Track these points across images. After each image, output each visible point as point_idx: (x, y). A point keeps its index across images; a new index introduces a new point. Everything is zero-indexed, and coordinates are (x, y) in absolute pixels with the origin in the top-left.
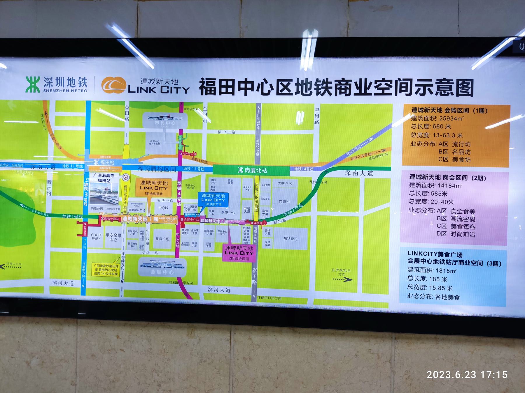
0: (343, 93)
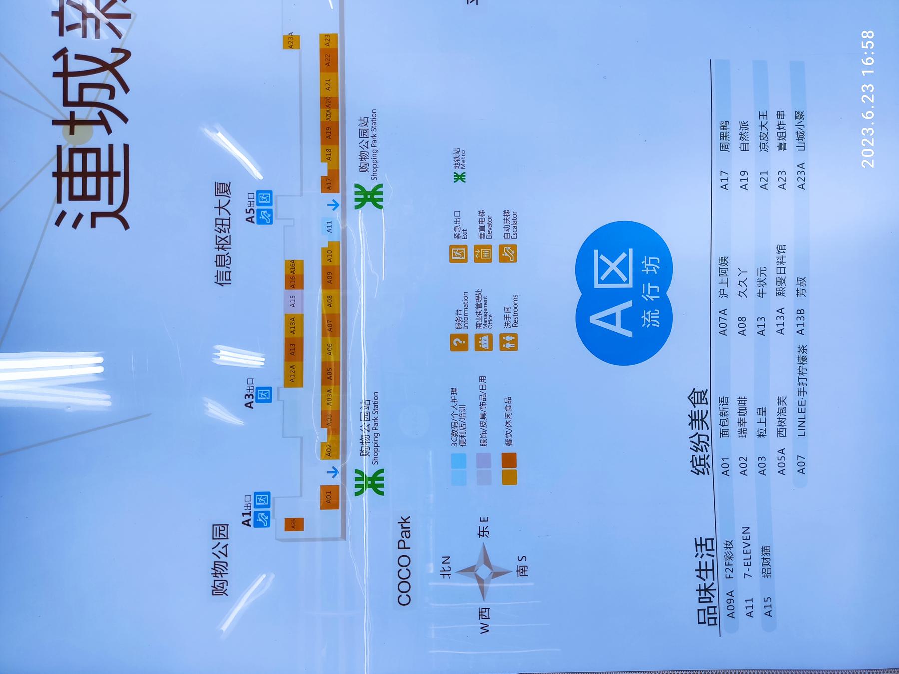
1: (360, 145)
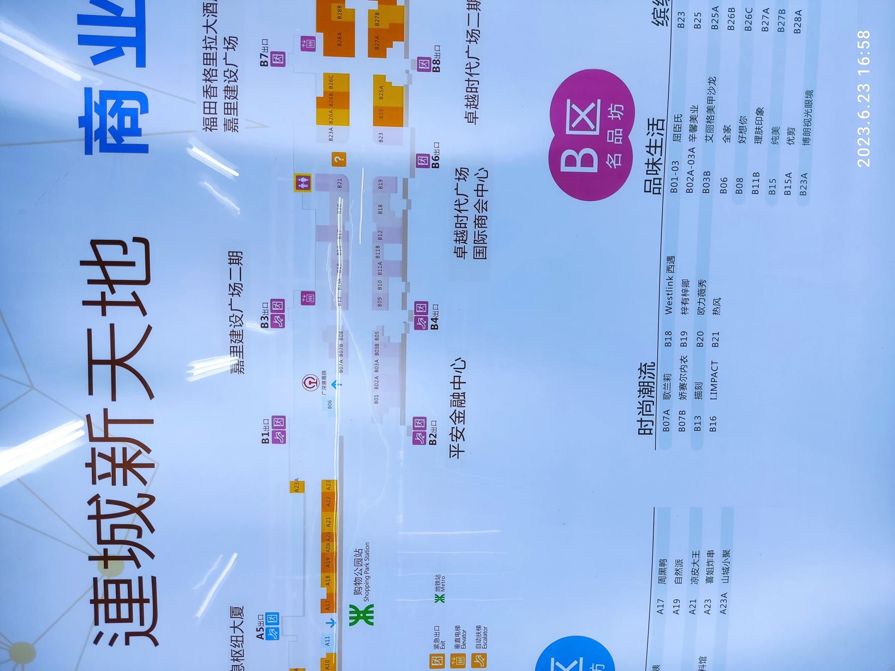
0: (135, 121)
1: (355, 572)
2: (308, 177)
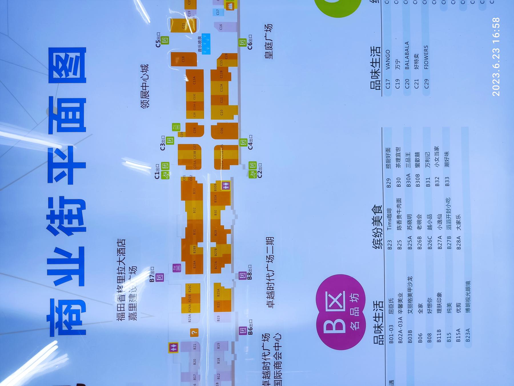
0: (78, 317)
2: (177, 344)
